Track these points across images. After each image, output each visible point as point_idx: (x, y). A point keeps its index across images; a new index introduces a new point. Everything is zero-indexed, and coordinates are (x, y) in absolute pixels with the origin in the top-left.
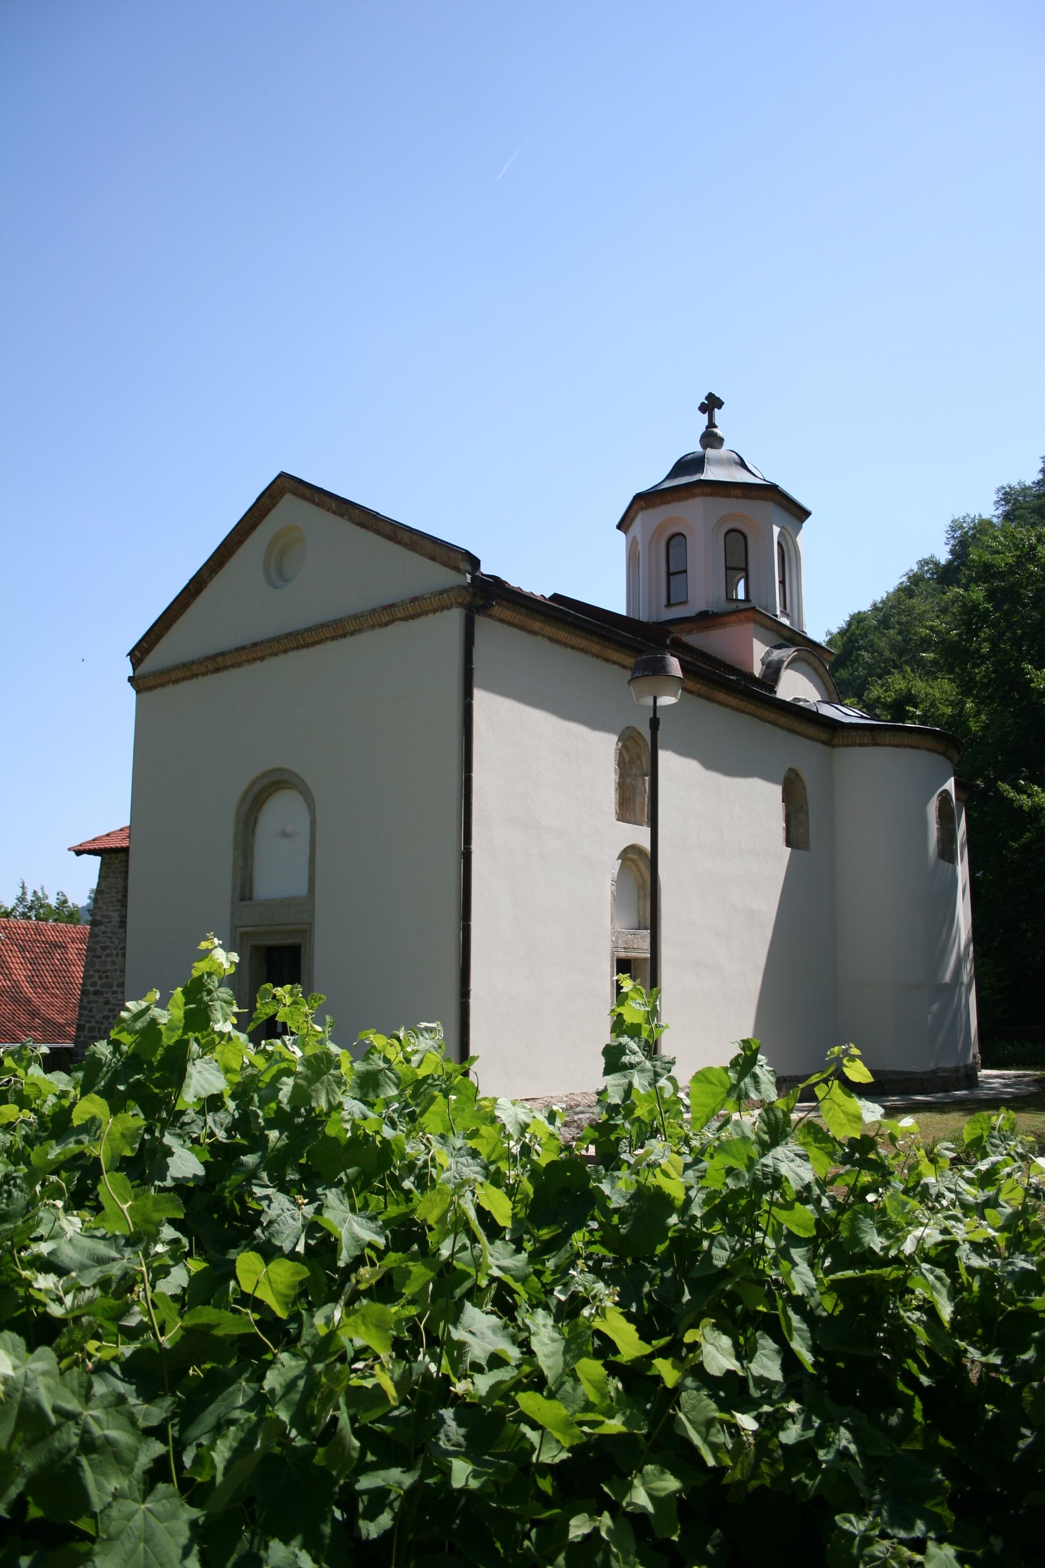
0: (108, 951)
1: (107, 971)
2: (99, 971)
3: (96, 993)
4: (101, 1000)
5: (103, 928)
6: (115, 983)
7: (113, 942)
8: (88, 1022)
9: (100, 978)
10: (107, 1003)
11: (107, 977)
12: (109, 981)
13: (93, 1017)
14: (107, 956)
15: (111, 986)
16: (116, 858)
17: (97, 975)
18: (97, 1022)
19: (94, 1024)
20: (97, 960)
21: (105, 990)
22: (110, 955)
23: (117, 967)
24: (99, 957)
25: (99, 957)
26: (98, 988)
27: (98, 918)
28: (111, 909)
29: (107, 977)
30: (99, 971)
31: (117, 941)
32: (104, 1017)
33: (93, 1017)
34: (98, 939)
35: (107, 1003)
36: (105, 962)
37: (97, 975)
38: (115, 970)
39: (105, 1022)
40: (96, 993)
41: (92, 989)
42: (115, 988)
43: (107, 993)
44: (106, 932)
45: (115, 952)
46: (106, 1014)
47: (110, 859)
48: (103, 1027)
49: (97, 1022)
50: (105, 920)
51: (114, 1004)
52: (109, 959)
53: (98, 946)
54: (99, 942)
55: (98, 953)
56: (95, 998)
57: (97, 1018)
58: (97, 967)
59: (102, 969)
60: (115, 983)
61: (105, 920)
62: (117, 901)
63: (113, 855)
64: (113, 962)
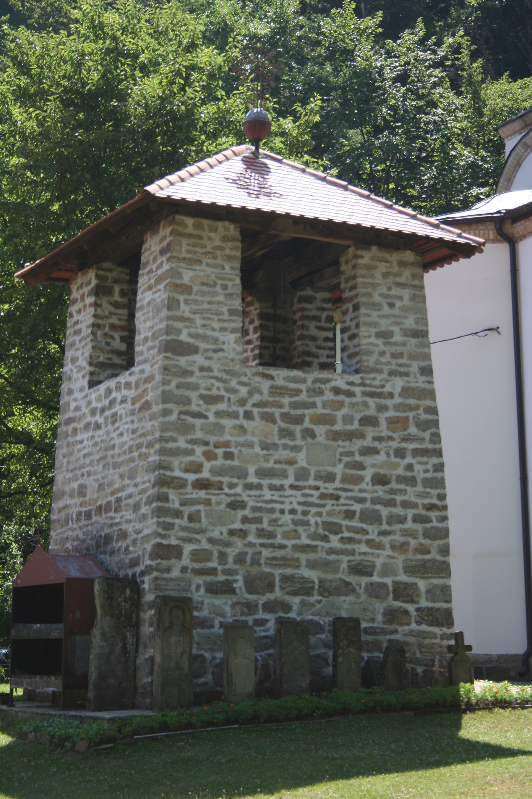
0: (222, 406)
1: (227, 444)
2: (206, 444)
3: (201, 485)
4: (219, 500)
5: (199, 359)
6: (252, 470)
7: (235, 391)
8: (190, 540)
9: (210, 456)
10: (236, 505)
11: (228, 456)
12: (236, 463)
13: (202, 531)
14: (218, 414)
15: (243, 474)
16: (215, 230)
17: (199, 450)
18: (211, 541)
19: (205, 545)
20: (198, 422)
21: (225, 480)
22: (234, 415)
23: (249, 438)
24: (200, 415)
25: (200, 415)
26: (205, 474)
27: (184, 337)
28: (217, 325)
29: (228, 456)
30: (206, 444)
31: (244, 391)
32: (232, 533)
33: (202, 531)
34: (192, 380)
35: (236, 505)
36: (221, 428)
37: (199, 450)
38: (250, 445)
39: (239, 544)
40: (201, 485)
41: (191, 477)
42: (252, 479)
43: (232, 486)
44: (209, 369)
45: (241, 410)
46: (237, 526)
47: (197, 226)
48: (232, 552)
49: (211, 541)
50: (203, 346)
51: (254, 509)
52: (228, 423)
53: (193, 395)
54: (196, 387)
55: (194, 408)
56: (202, 494)
57: (215, 534)
58: (199, 435)
59: (213, 439)
60: (252, 470)
61: (203, 346)
62: (231, 312)
63: (205, 222)
64: (242, 429)
